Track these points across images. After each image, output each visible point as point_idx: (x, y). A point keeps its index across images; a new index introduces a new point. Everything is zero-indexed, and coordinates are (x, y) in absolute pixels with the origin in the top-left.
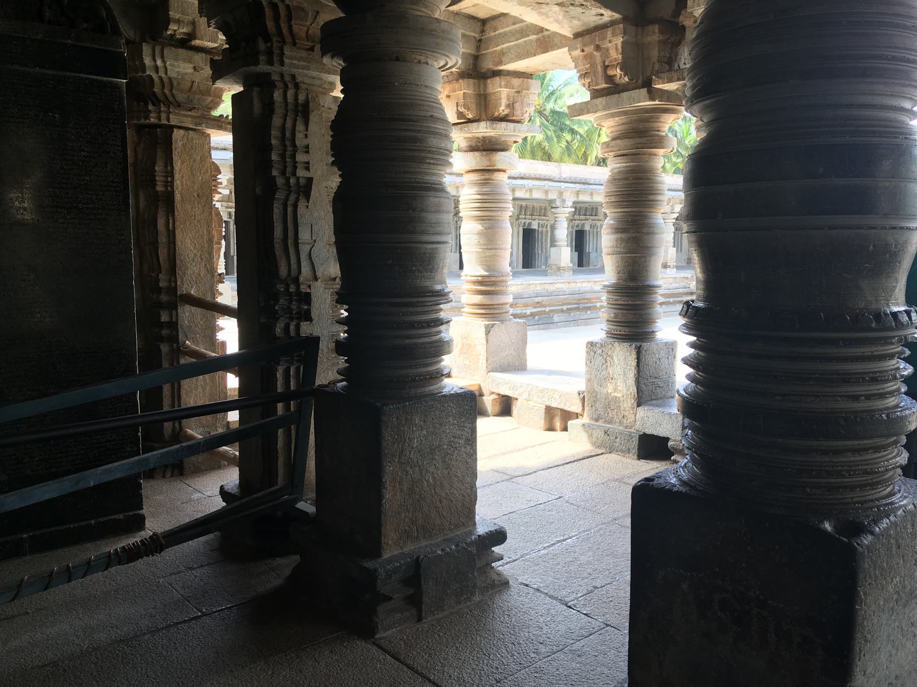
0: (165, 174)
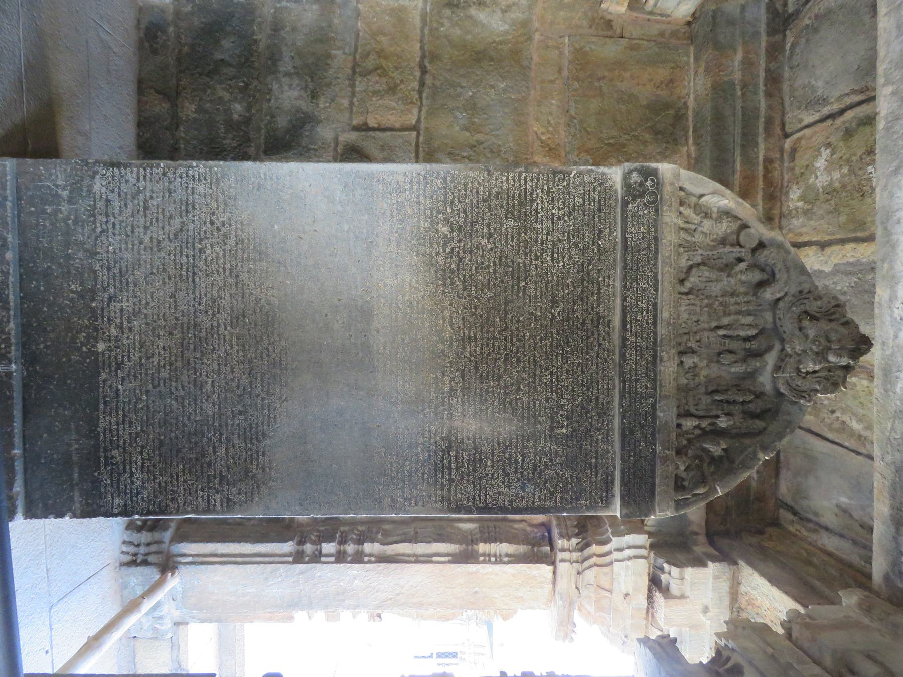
0: (498, 554)
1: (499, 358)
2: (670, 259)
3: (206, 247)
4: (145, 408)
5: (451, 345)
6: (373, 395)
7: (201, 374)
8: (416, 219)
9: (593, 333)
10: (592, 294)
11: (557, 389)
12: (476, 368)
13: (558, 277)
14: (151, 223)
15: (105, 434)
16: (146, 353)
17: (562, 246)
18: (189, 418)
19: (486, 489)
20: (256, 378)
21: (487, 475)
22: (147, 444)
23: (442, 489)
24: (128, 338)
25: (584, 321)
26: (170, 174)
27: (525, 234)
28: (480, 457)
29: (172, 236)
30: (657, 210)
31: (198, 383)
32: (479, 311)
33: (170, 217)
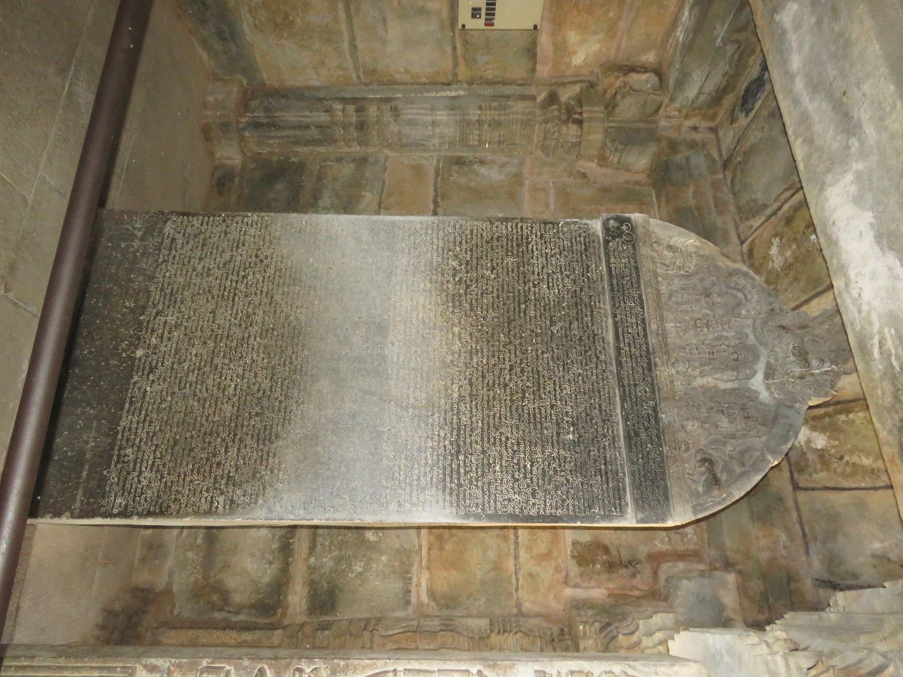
1: (505, 369)
2: (651, 282)
3: (249, 274)
4: (168, 409)
5: (459, 356)
6: (385, 401)
7: (226, 379)
8: (429, 255)
9: (590, 347)
10: (586, 316)
11: (561, 397)
12: (483, 377)
13: (554, 301)
14: (206, 256)
15: (123, 433)
16: (179, 359)
17: (555, 277)
18: (207, 418)
19: (495, 495)
20: (277, 383)
21: (496, 480)
22: (162, 443)
23: (451, 494)
24: (166, 346)
25: (581, 338)
26: (229, 222)
27: (524, 267)
28: (489, 461)
29: (221, 265)
30: (634, 247)
31: (222, 386)
32: (484, 328)
33: (223, 251)
